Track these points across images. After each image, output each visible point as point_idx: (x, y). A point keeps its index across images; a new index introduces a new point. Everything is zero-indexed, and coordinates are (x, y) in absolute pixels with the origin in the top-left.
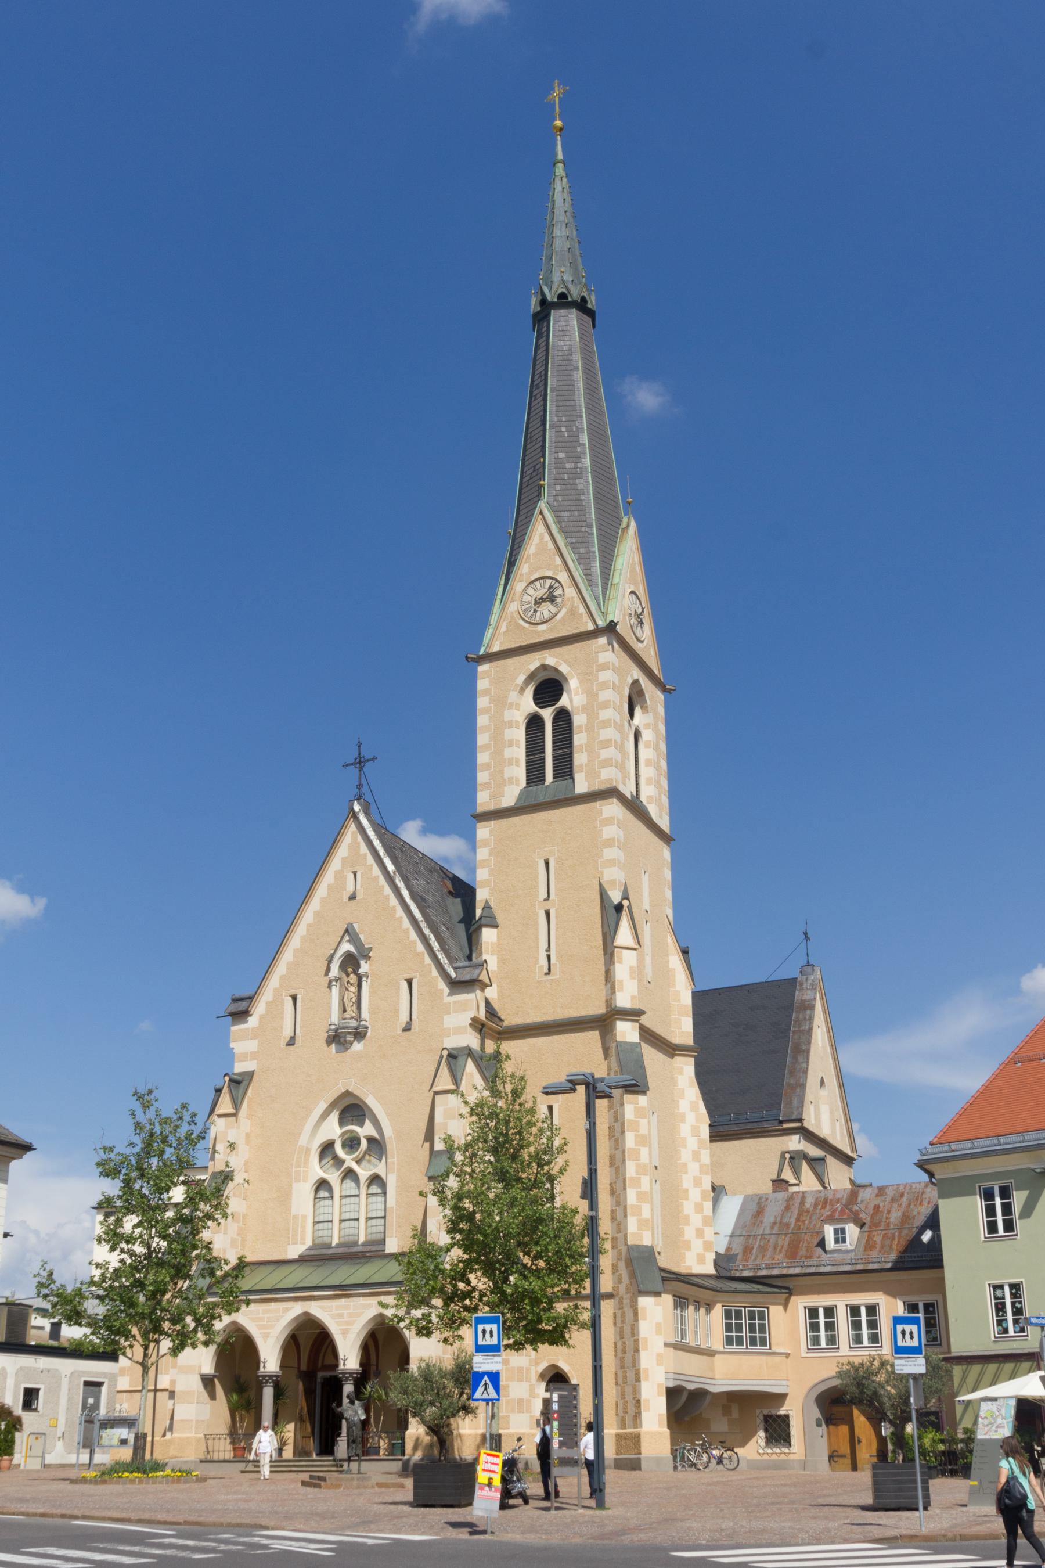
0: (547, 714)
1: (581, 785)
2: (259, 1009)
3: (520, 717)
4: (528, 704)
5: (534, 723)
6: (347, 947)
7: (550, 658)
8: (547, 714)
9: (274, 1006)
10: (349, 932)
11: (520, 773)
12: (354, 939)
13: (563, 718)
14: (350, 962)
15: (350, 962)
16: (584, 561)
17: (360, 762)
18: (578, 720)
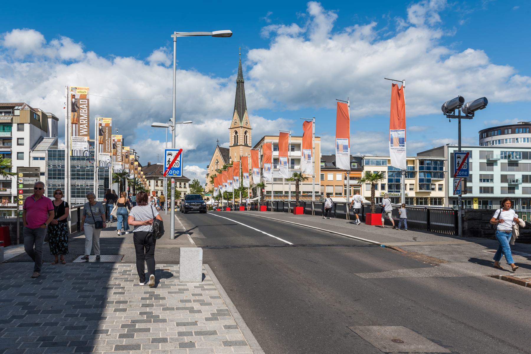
0: (236, 136)
1: (238, 144)
2: (210, 167)
3: (234, 136)
4: (235, 134)
5: (235, 136)
6: (217, 161)
7: (236, 129)
8: (236, 136)
9: (211, 167)
10: (217, 160)
11: (234, 142)
12: (217, 161)
13: (237, 136)
14: (217, 163)
15: (217, 163)
16: (240, 118)
17: (218, 141)
18: (238, 137)
